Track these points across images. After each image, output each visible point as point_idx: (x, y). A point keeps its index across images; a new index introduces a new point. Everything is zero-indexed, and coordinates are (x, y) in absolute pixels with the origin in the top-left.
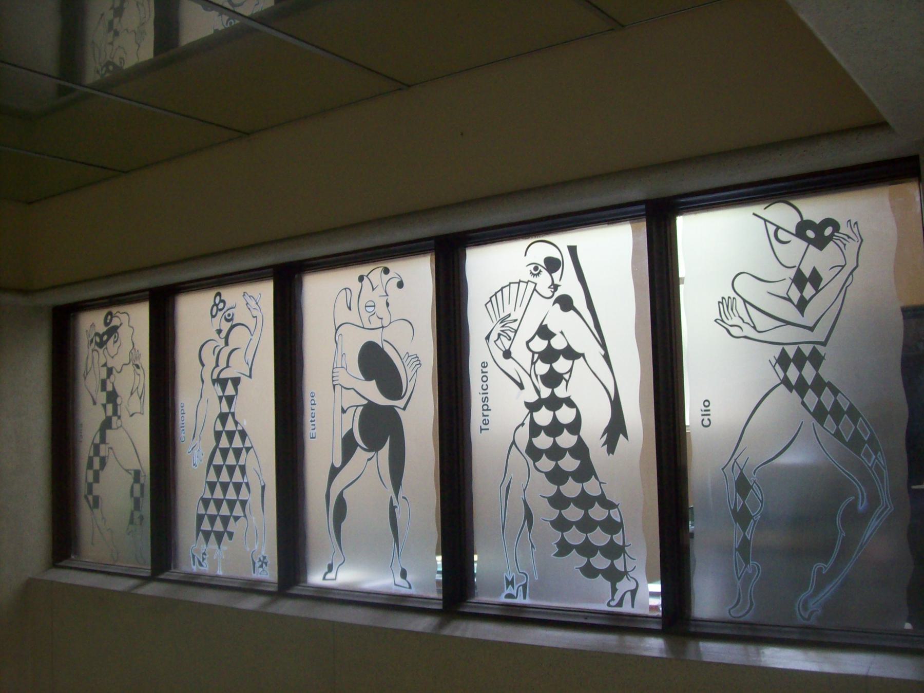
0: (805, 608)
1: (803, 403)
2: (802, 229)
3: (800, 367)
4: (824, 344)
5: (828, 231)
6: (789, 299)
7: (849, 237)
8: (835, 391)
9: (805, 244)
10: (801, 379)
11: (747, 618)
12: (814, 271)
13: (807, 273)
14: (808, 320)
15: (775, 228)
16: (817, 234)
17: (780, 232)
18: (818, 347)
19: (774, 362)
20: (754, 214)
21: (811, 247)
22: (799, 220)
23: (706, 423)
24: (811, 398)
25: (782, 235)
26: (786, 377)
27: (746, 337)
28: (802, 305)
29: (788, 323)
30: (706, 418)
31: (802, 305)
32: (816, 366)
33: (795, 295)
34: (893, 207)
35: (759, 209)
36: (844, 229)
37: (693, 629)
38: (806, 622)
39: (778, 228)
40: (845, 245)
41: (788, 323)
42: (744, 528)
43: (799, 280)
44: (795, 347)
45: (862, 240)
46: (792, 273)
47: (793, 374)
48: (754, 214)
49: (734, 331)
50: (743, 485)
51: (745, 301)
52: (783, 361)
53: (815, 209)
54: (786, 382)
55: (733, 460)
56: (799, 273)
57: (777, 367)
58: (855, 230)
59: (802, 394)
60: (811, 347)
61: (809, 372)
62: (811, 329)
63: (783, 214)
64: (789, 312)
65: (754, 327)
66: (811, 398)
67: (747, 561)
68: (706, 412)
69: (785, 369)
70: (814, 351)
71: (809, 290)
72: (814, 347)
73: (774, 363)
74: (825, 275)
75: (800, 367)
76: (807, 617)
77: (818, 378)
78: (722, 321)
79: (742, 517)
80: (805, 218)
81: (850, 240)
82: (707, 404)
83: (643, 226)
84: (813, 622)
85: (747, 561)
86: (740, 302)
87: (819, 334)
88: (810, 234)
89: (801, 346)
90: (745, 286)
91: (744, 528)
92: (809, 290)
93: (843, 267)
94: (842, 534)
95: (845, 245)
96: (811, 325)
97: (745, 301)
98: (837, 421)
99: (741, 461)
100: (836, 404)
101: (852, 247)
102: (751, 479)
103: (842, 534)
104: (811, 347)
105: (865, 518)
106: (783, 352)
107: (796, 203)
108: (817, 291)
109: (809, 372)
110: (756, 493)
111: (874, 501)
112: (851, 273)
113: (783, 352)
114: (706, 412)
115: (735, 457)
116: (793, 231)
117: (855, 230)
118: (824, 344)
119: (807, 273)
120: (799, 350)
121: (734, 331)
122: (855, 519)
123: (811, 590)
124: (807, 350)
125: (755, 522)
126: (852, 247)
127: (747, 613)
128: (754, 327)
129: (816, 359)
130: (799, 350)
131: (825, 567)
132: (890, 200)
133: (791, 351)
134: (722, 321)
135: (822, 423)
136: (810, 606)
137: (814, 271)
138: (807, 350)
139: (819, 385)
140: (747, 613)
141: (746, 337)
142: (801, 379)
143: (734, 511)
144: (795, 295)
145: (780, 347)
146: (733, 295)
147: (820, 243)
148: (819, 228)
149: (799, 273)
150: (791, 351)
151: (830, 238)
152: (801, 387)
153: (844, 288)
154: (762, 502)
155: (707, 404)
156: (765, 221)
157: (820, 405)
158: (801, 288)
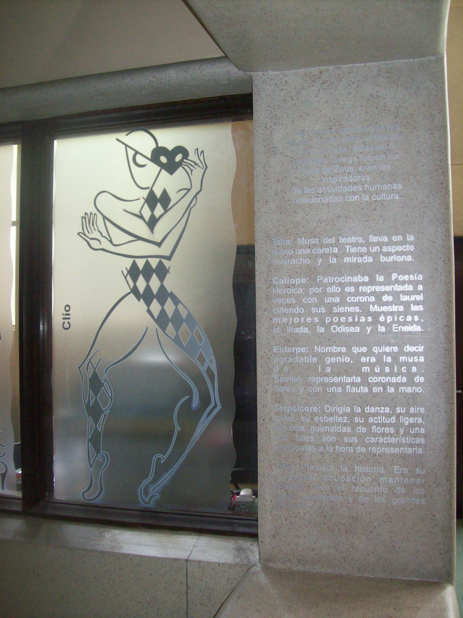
0: (146, 492)
1: (149, 311)
2: (157, 154)
3: (148, 279)
4: (169, 258)
5: (179, 158)
6: (141, 217)
7: (196, 164)
8: (176, 301)
9: (158, 168)
10: (148, 288)
11: (98, 501)
12: (165, 193)
13: (158, 194)
14: (158, 236)
15: (134, 152)
16: (168, 159)
17: (138, 156)
18: (165, 262)
19: (126, 273)
20: (117, 140)
21: (163, 171)
22: (154, 146)
23: (66, 326)
24: (155, 307)
25: (140, 160)
26: (135, 286)
27: (103, 250)
28: (152, 223)
29: (139, 238)
30: (66, 321)
31: (152, 223)
32: (162, 278)
33: (147, 213)
34: (234, 139)
35: (122, 136)
36: (192, 156)
37: (49, 512)
38: (147, 506)
39: (137, 153)
40: (192, 170)
41: (139, 238)
42: (96, 420)
43: (151, 200)
44: (144, 260)
45: (207, 167)
46: (145, 193)
47: (141, 284)
48: (117, 140)
49: (94, 244)
50: (95, 383)
51: (104, 217)
52: (134, 272)
53: (169, 137)
54: (135, 291)
55: (88, 360)
56: (152, 193)
57: (129, 278)
58: (201, 158)
59: (148, 303)
60: (157, 260)
61: (155, 284)
62: (159, 244)
63: (142, 141)
64: (141, 229)
65: (111, 241)
66: (155, 307)
67: (98, 451)
68: (67, 316)
69: (135, 279)
70: (160, 264)
71: (159, 210)
72: (160, 261)
73: (125, 274)
74: (174, 197)
75: (148, 279)
76: (147, 501)
77: (162, 288)
78: (84, 234)
79: (95, 411)
80: (160, 145)
81: (196, 167)
82: (67, 308)
83: (20, 145)
84: (152, 505)
85: (98, 451)
86: (100, 217)
87: (165, 250)
88: (163, 159)
89: (150, 260)
90: (108, 206)
91: (96, 420)
92: (159, 210)
93: (189, 190)
94: (178, 429)
95: (192, 170)
96: (159, 241)
97: (104, 217)
98: (177, 328)
99: (95, 361)
100: (176, 312)
101: (197, 172)
102: (103, 377)
103: (178, 429)
104: (157, 260)
105: (199, 413)
106: (134, 265)
107: (154, 132)
108: (166, 211)
109: (155, 284)
110: (107, 390)
111: (205, 399)
112: (195, 196)
113: (134, 265)
114: (67, 316)
115: (89, 357)
116: (149, 156)
117: (201, 158)
118: (169, 258)
119: (158, 194)
120: (147, 262)
121: (94, 244)
122: (191, 416)
123: (150, 478)
124: (154, 263)
125: (105, 416)
126: (197, 172)
127: (98, 496)
128: (111, 241)
129: (162, 272)
130: (147, 262)
131: (164, 458)
132: (232, 133)
133: (141, 263)
134: (84, 234)
135: (164, 329)
136: (150, 493)
137: (165, 193)
138: (154, 263)
139: (163, 295)
140: (98, 496)
141: (103, 250)
142: (148, 288)
143: (88, 405)
144: (147, 213)
145: (131, 260)
146: (94, 211)
147: (171, 168)
148: (171, 154)
149: (152, 193)
150: (141, 263)
151: (180, 164)
152: (147, 297)
153: (189, 208)
154: (111, 398)
155: (67, 308)
156: (126, 146)
157: (163, 312)
158: (152, 208)
